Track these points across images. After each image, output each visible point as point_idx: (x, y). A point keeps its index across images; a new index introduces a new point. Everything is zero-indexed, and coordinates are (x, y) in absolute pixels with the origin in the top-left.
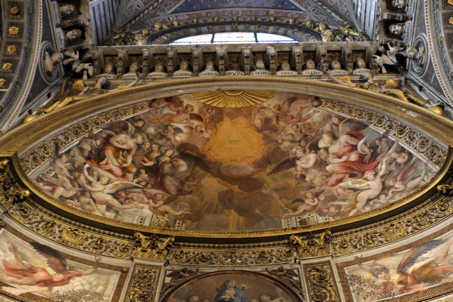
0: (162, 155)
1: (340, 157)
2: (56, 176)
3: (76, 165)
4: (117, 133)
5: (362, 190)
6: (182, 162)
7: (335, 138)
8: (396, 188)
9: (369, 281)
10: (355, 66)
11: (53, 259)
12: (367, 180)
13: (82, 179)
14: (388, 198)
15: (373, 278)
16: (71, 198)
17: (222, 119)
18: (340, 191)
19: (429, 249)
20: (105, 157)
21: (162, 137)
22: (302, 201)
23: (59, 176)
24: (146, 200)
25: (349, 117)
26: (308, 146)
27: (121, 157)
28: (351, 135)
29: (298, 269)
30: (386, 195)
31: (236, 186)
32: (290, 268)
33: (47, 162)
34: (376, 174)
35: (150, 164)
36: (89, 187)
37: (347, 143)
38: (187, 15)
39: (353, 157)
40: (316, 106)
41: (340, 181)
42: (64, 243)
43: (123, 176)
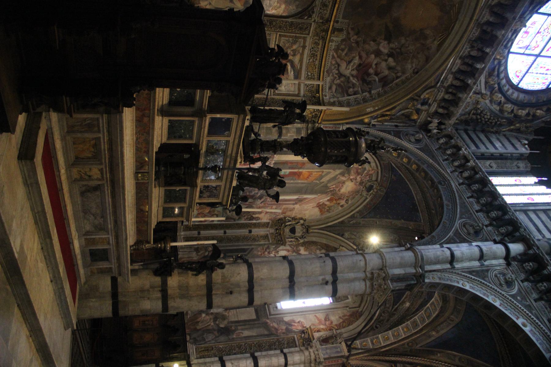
1: (376, 64)
5: (347, 65)
7: (390, 68)
8: (337, 80)
9: (292, 47)
10: (439, 106)
12: (353, 70)
14: (334, 74)
15: (292, 49)
18: (354, 55)
25: (394, 82)
26: (394, 52)
28: (386, 77)
29: (311, 20)
30: (336, 74)
32: (313, 16)
34: (352, 76)
37: (383, 72)
39: (371, 71)
40: (414, 70)
41: (360, 57)
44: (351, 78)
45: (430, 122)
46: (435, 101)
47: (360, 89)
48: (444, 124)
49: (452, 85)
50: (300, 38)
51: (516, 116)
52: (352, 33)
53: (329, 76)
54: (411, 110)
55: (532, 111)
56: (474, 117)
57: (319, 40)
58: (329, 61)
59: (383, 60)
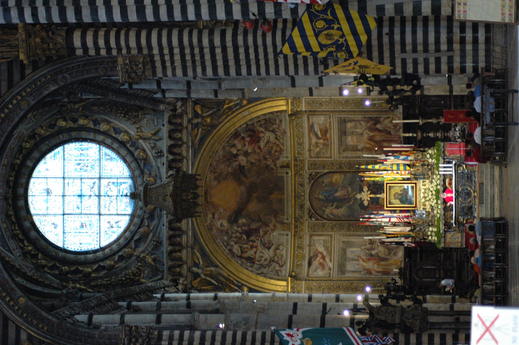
0: (237, 231)
1: (245, 145)
2: (272, 271)
3: (259, 266)
4: (234, 253)
5: (269, 139)
6: (240, 221)
7: (234, 146)
10: (181, 124)
11: (313, 259)
12: (263, 137)
13: (266, 263)
16: (279, 264)
17: (213, 202)
18: (266, 148)
19: (314, 128)
20: (248, 257)
21: (227, 233)
22: (268, 166)
23: (270, 270)
24: (268, 235)
27: (246, 250)
31: (254, 195)
33: (269, 275)
34: (263, 132)
35: (245, 237)
36: (269, 259)
38: (9, 240)
39: (248, 139)
41: (259, 148)
42: (304, 258)
43: (256, 247)
44: (263, 130)
45: (181, 107)
46: (187, 128)
47: (255, 124)
48: (171, 110)
49: (180, 146)
50: (314, 157)
51: (86, 117)
52: (272, 166)
53: (284, 130)
54: (204, 115)
55: (71, 124)
56: (136, 114)
57: (299, 157)
58: (288, 143)
59: (241, 150)
